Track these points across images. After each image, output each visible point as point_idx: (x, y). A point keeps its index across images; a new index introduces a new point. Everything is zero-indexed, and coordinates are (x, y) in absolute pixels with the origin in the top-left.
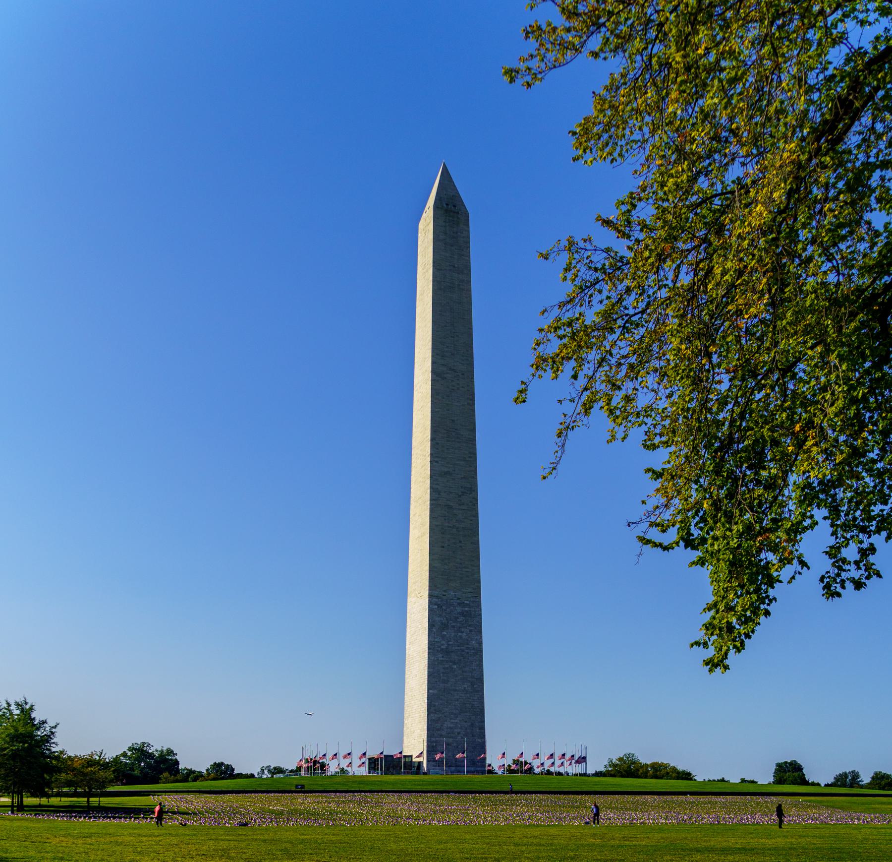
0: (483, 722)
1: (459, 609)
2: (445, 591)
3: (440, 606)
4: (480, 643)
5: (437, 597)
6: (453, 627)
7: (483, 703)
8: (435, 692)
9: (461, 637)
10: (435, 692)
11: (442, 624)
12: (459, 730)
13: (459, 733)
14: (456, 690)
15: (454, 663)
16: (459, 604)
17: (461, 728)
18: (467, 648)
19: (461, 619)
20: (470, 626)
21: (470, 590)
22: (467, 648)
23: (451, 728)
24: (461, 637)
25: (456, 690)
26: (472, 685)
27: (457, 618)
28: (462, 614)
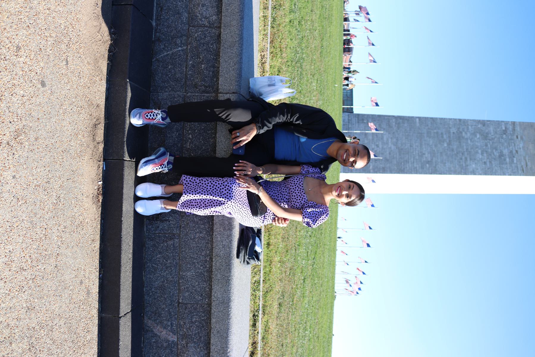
0: (391, 172)
1: (506, 152)
2: (522, 138)
3: (505, 132)
4: (474, 173)
5: (514, 130)
6: (486, 145)
7: (411, 173)
8: (418, 125)
9: (477, 152)
10: (418, 125)
11: (487, 134)
12: (380, 146)
13: (377, 146)
14: (421, 145)
15: (449, 144)
16: (511, 152)
17: (383, 148)
18: (466, 159)
19: (496, 154)
20: (490, 162)
21: (529, 164)
22: (466, 159)
23: (382, 138)
24: (477, 152)
25: (421, 145)
26: (428, 162)
27: (496, 150)
28: (501, 155)
